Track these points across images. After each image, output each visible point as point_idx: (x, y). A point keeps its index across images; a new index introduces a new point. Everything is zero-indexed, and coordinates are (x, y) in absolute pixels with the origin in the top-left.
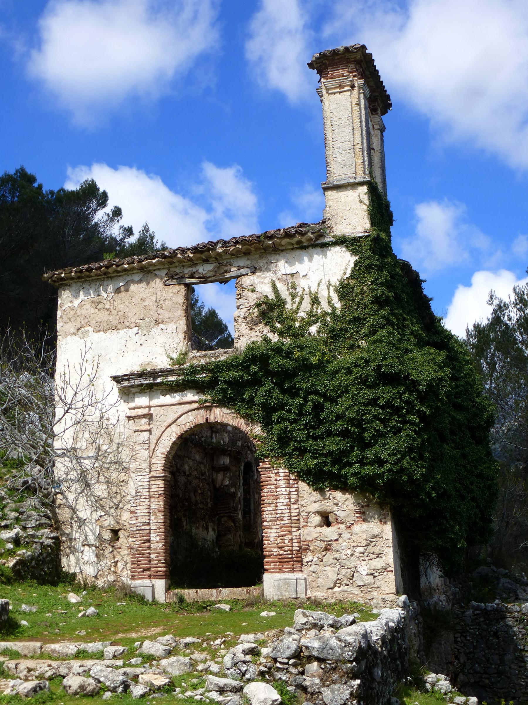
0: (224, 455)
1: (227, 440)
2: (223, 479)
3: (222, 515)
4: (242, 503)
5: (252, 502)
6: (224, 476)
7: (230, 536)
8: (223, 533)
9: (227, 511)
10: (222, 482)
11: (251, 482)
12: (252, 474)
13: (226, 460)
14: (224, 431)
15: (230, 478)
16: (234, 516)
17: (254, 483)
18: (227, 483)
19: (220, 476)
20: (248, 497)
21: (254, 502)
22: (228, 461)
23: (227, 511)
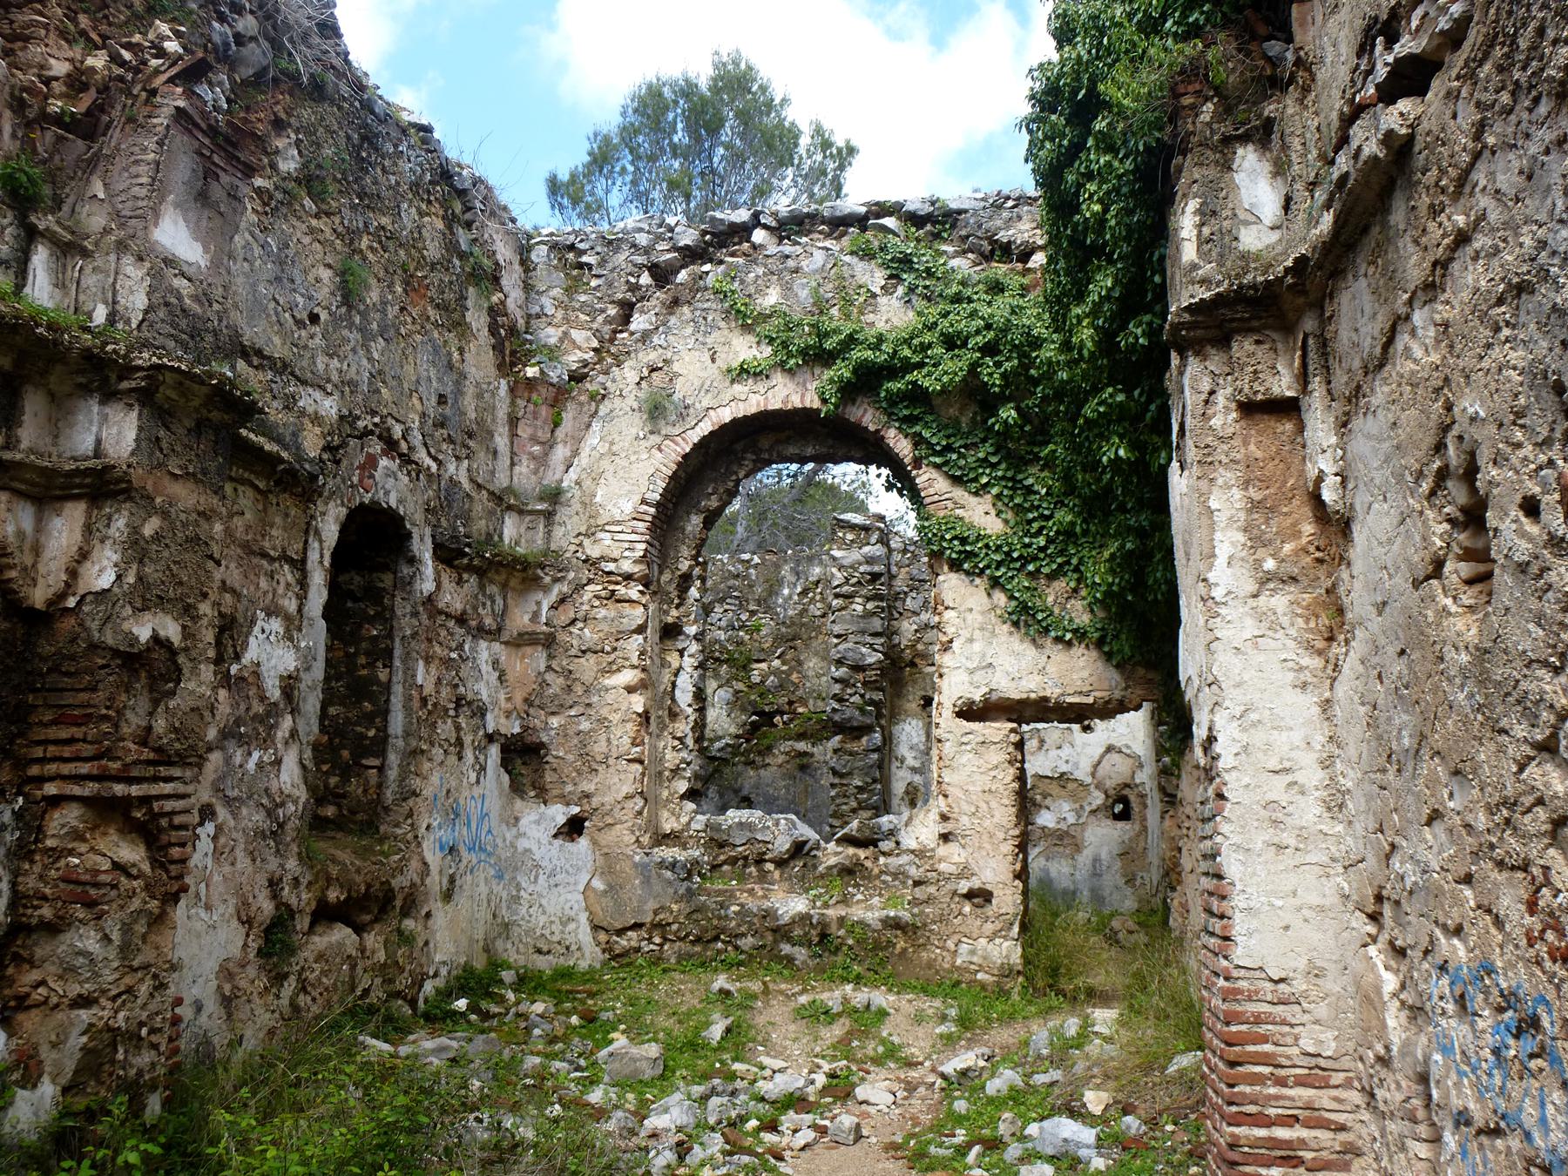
0: (109, 396)
1: (140, 301)
2: (83, 555)
3: (51, 789)
4: (311, 704)
5: (397, 701)
6: (88, 530)
7: (90, 941)
8: (47, 912)
9: (85, 768)
10: (73, 574)
11: (402, 608)
12: (406, 570)
13: (115, 432)
14: (122, 247)
15: (136, 549)
16: (146, 800)
17: (415, 614)
18: (106, 580)
19: (64, 529)
20: (383, 675)
21: (408, 699)
22: (131, 435)
23: (85, 768)
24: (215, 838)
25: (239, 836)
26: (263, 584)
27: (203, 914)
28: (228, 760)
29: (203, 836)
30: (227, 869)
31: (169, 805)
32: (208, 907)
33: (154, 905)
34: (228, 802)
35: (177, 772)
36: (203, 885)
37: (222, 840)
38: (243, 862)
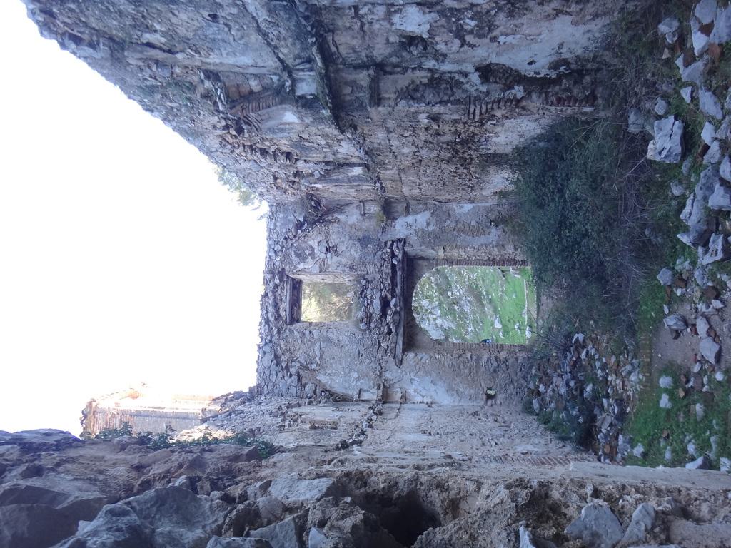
16: (481, 114)
24: (507, 35)
25: (509, 23)
26: (377, 26)
27: (542, 36)
28: (471, 32)
29: (505, 41)
30: (525, 27)
31: (484, 110)
32: (540, 34)
33: (517, 110)
34: (490, 31)
35: (472, 110)
36: (528, 38)
37: (509, 31)
38: (524, 20)
